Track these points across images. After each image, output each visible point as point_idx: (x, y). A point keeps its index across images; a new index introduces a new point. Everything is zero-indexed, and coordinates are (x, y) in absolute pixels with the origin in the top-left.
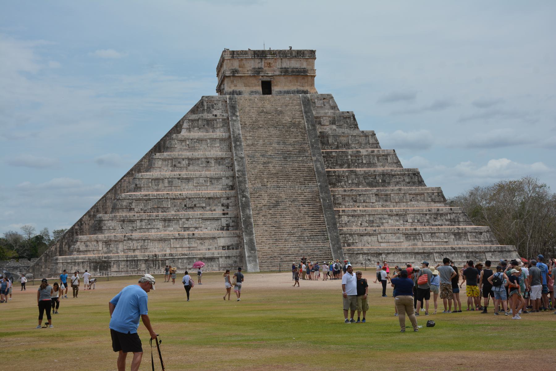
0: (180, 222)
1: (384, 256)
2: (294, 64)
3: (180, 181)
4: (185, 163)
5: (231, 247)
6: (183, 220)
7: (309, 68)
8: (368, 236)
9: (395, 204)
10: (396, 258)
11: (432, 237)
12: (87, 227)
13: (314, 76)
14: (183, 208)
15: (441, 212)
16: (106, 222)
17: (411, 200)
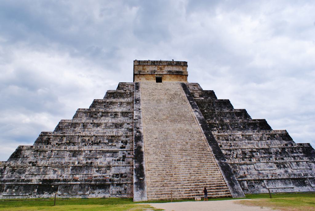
1: (265, 182)
2: (175, 69)
3: (92, 125)
4: (101, 114)
5: (123, 175)
6: (86, 152)
7: (184, 71)
8: (246, 166)
9: (257, 141)
10: (277, 185)
11: (298, 165)
13: (187, 75)
14: (90, 144)
15: (295, 147)
16: (23, 151)
17: (268, 139)
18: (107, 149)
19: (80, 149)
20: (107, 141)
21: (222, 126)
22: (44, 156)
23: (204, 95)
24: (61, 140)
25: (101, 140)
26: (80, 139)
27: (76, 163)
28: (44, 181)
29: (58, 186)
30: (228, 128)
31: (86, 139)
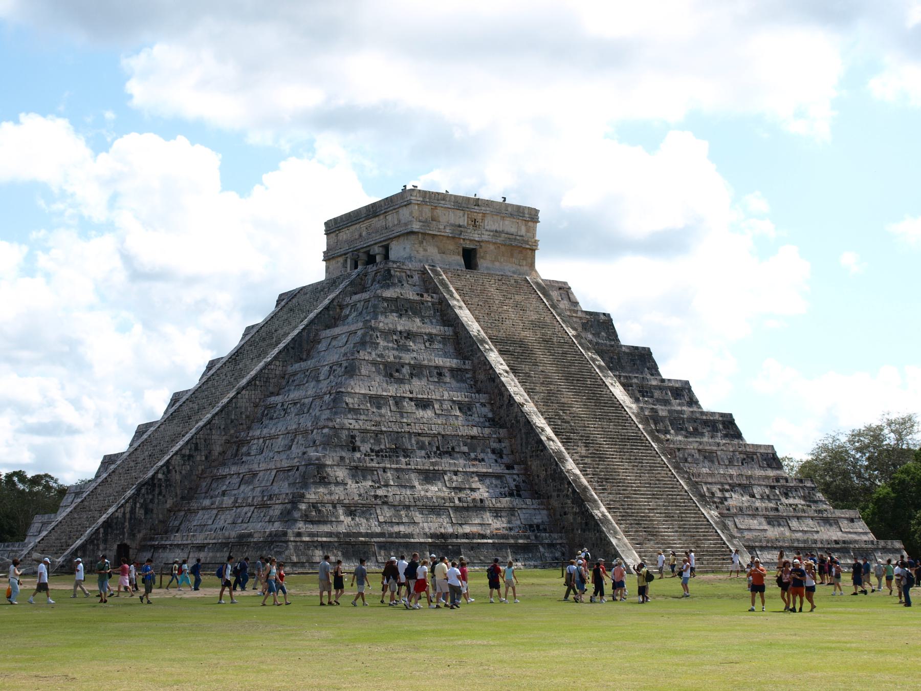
0: (446, 478)
2: (509, 226)
4: (406, 370)
5: (541, 527)
12: (178, 477)
13: (533, 251)
18: (485, 470)
19: (436, 468)
20: (466, 449)
21: (655, 424)
22: (373, 481)
23: (591, 326)
24: (378, 441)
25: (455, 444)
26: (413, 441)
27: (457, 502)
28: (432, 536)
29: (459, 545)
30: (667, 432)
31: (423, 443)
